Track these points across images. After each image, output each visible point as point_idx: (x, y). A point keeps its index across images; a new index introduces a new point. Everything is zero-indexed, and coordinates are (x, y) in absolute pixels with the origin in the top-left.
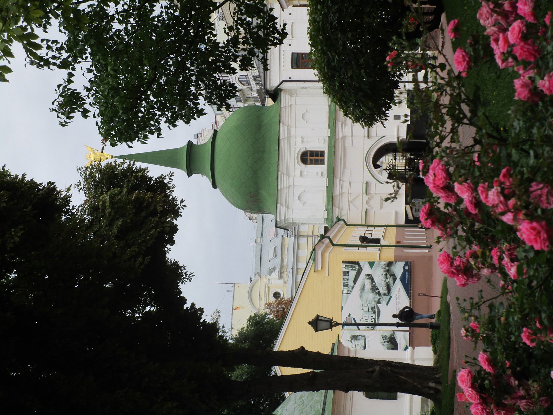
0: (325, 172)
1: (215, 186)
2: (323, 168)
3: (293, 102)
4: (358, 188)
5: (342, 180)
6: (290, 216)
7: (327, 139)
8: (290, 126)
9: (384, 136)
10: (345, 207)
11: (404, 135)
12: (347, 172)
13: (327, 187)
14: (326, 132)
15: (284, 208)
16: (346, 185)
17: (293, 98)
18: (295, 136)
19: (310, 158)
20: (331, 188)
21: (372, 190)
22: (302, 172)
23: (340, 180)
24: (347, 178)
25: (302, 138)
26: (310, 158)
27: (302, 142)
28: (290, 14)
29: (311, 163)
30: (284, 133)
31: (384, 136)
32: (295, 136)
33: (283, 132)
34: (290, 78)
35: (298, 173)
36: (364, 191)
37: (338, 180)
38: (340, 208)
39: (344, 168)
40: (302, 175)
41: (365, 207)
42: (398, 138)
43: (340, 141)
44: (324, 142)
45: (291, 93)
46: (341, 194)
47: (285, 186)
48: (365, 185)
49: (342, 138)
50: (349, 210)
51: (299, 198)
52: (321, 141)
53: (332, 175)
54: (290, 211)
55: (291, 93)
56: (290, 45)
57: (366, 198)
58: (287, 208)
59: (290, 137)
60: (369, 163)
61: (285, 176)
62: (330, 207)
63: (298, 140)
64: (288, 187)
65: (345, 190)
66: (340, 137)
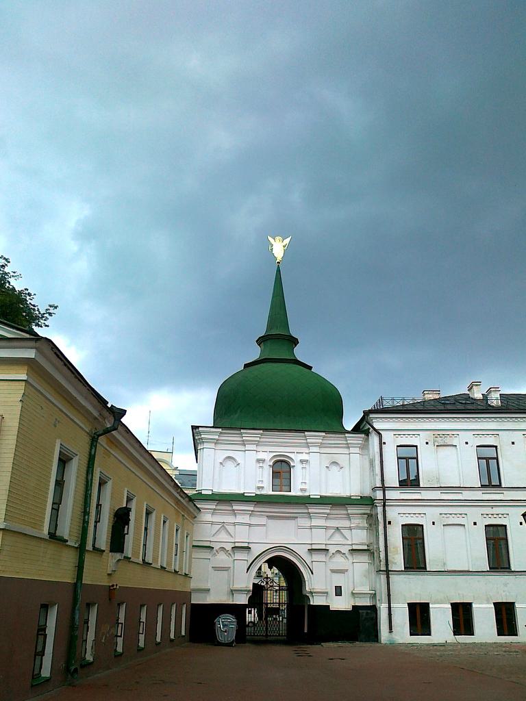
0: (264, 492)
1: (246, 366)
3: (352, 450)
4: (242, 536)
5: (252, 513)
6: (206, 445)
7: (307, 494)
8: (321, 446)
9: (312, 573)
10: (217, 519)
11: (316, 601)
12: (263, 520)
13: (243, 494)
14: (315, 493)
15: (217, 437)
16: (245, 519)
17: (357, 450)
18: (309, 453)
19: (281, 470)
21: (240, 555)
22: (264, 461)
23: (252, 511)
24: (255, 521)
26: (281, 470)
27: (302, 461)
28: (467, 443)
30: (314, 438)
31: (312, 573)
32: (309, 453)
33: (315, 436)
34: (385, 443)
35: (261, 456)
36: (237, 545)
37: (252, 509)
38: (214, 512)
40: (258, 461)
41: (217, 546)
42: (311, 593)
43: (306, 511)
44: (302, 490)
45: (365, 447)
46: (234, 513)
48: (246, 545)
49: (309, 513)
50: (212, 523)
51: (229, 458)
52: (303, 487)
53: (259, 500)
54: (212, 446)
55: (365, 447)
56: (427, 443)
57: (229, 547)
58: (217, 442)
59: (308, 445)
60: (276, 550)
61: (258, 439)
62: (217, 498)
63: (305, 457)
64: (244, 443)
65: (240, 519)
66: (310, 511)
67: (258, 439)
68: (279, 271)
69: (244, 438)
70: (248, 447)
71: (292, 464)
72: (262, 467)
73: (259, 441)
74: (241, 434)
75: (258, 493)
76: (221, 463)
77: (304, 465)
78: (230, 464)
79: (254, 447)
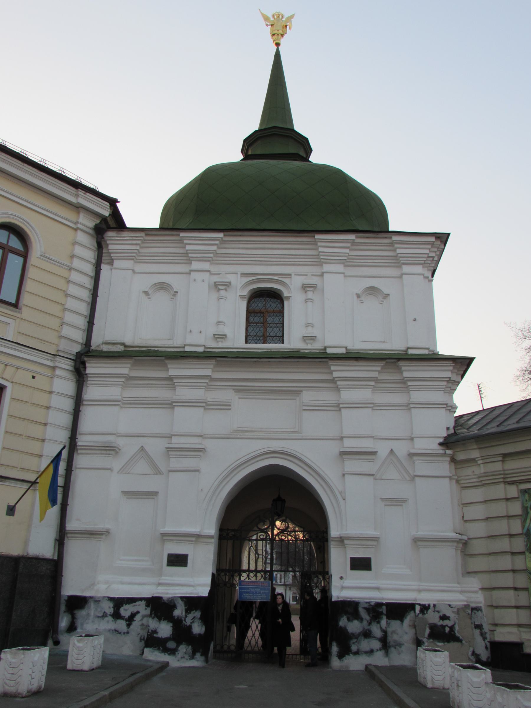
2: (236, 339)
7: (317, 346)
19: (265, 305)
20: (182, 356)
22: (228, 285)
25: (314, 287)
26: (265, 305)
27: (305, 287)
29: (249, 312)
39: (237, 390)
40: (216, 286)
44: (306, 338)
47: (188, 247)
51: (163, 287)
52: (310, 332)
67: (215, 248)
68: (277, 56)
69: (188, 247)
70: (195, 265)
71: (286, 293)
72: (225, 298)
73: (216, 254)
74: (181, 241)
75: (213, 344)
76: (146, 293)
77: (310, 295)
78: (162, 297)
79: (206, 266)
